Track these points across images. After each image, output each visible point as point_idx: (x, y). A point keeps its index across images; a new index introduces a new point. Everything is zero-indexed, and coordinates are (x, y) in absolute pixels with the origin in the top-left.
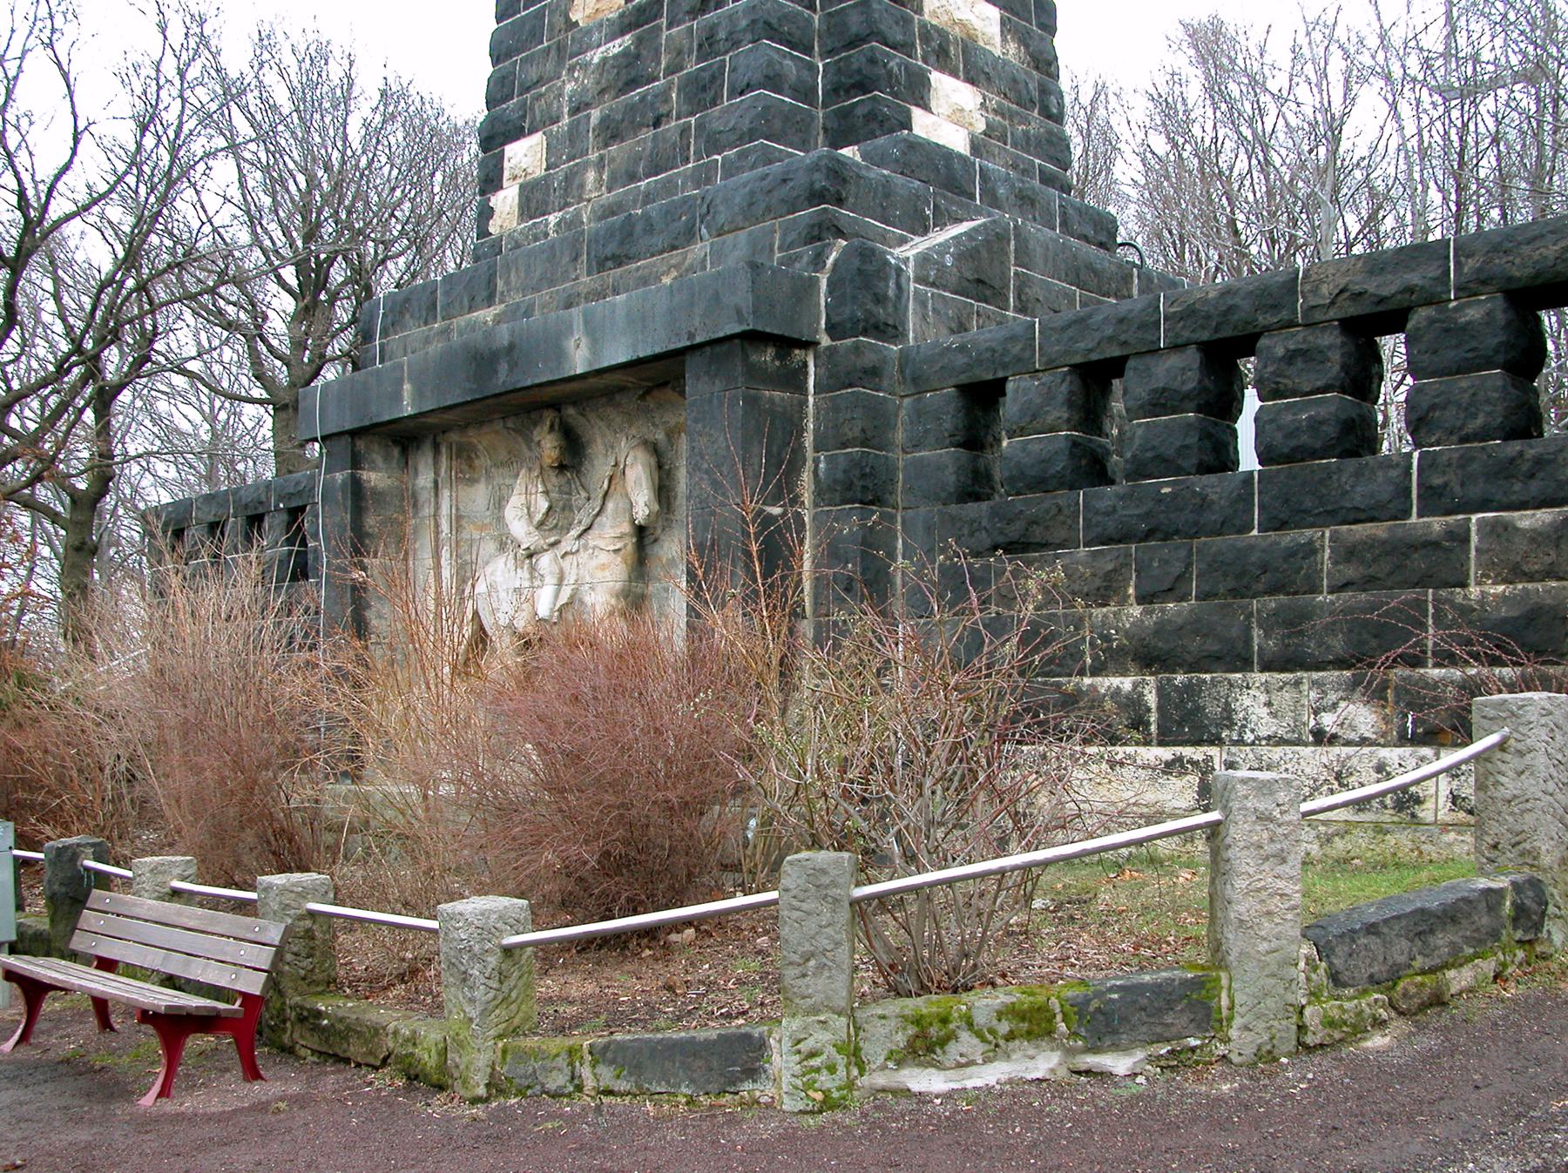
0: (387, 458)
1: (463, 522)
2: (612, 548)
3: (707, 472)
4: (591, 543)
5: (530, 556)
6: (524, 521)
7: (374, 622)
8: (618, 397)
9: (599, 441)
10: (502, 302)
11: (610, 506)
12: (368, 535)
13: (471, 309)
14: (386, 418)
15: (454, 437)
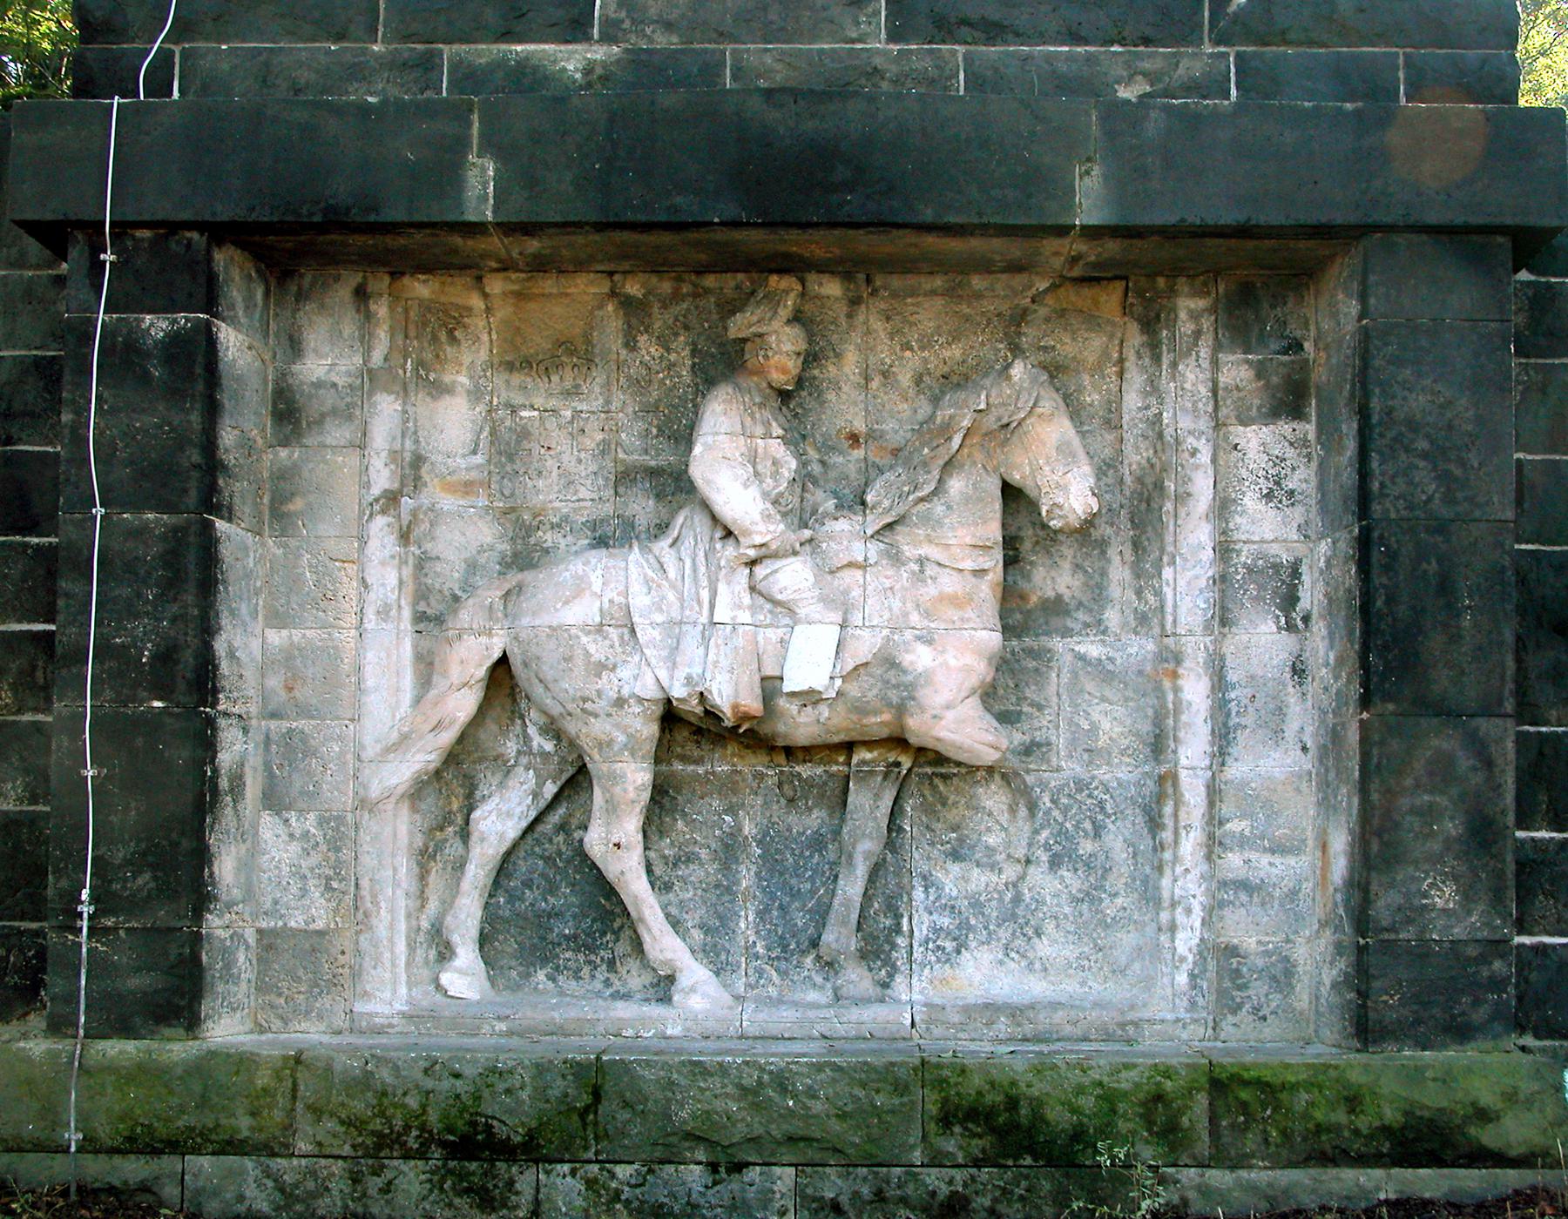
0: (249, 305)
1: (424, 471)
2: (968, 565)
3: (1425, 455)
4: (909, 551)
5: (752, 563)
6: (754, 491)
7: (225, 667)
8: (978, 282)
9: (851, 358)
10: (607, 39)
11: (956, 485)
12: (225, 468)
13: (507, 36)
14: (395, 213)
15: (421, 288)
